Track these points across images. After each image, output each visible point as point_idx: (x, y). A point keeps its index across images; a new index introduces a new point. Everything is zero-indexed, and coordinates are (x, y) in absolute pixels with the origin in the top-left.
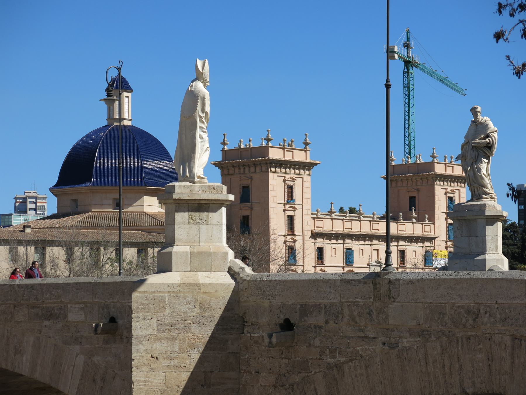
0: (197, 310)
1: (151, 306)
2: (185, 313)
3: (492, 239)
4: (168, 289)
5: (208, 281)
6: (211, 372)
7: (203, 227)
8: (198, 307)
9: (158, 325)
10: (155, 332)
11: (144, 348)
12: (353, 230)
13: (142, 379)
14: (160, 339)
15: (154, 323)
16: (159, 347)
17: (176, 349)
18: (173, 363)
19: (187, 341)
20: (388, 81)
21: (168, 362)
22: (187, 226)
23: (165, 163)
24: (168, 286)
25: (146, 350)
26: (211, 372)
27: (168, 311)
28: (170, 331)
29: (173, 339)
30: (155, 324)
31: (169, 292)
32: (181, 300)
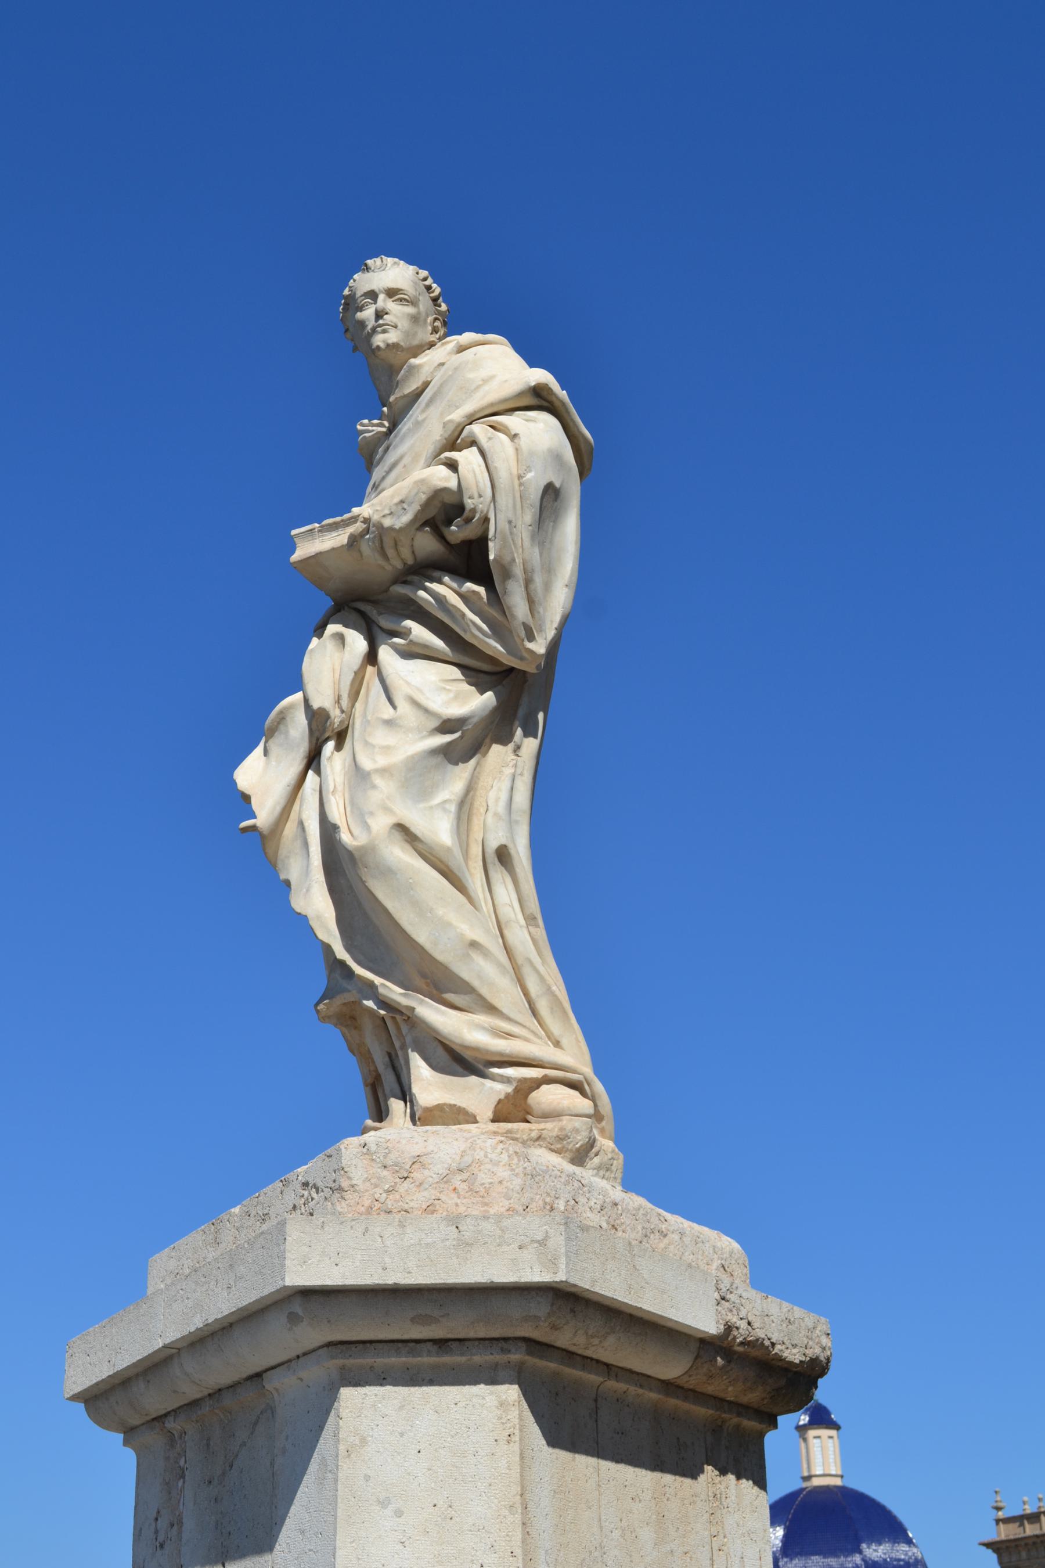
23: (904, 1547)
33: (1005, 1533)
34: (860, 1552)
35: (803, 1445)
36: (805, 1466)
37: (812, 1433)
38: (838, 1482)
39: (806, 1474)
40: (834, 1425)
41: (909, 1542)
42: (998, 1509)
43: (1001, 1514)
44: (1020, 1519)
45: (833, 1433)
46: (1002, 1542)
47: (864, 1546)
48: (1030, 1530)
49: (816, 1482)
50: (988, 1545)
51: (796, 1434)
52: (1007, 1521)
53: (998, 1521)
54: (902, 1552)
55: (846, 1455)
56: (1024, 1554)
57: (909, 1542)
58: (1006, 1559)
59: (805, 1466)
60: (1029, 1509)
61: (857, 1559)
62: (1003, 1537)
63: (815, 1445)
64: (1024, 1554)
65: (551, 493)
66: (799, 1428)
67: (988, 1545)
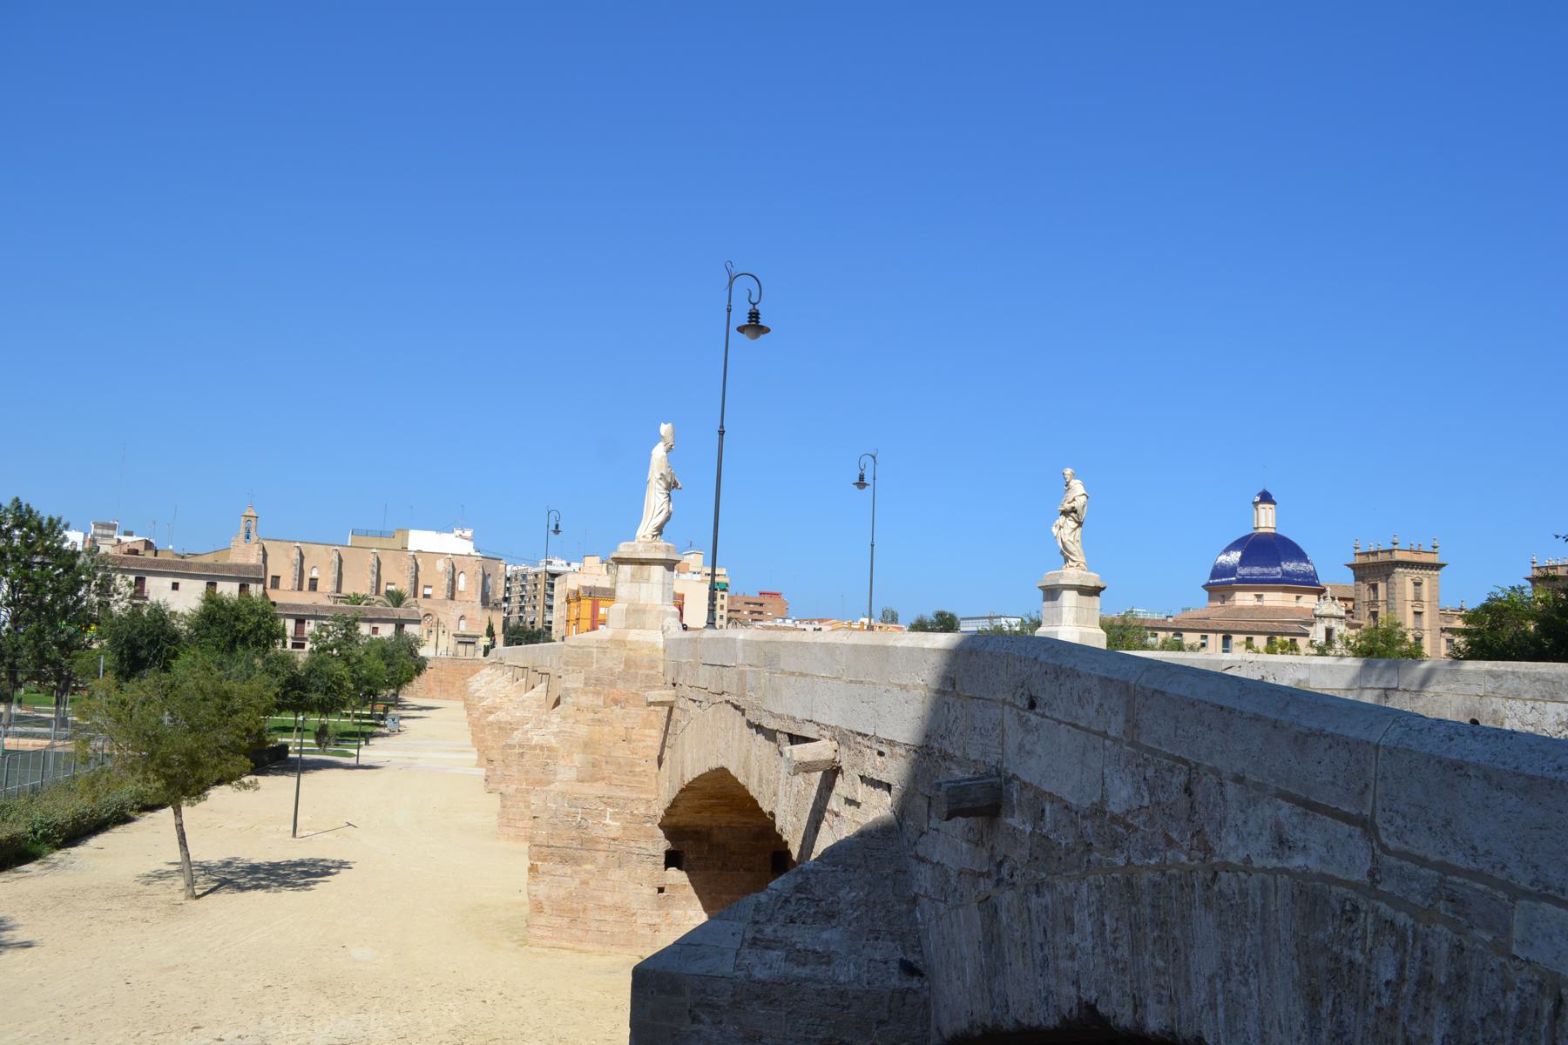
0: (622, 666)
1: (580, 660)
2: (611, 669)
3: (1069, 610)
4: (597, 645)
5: (640, 638)
6: (633, 728)
7: (644, 585)
8: (623, 664)
9: (586, 679)
10: (582, 686)
11: (571, 700)
12: (158, 558)
13: (569, 730)
14: (586, 693)
15: (582, 676)
16: (585, 700)
17: (601, 704)
18: (597, 716)
19: (611, 697)
20: (722, 427)
21: (591, 715)
22: (629, 585)
23: (1304, 564)
24: (597, 642)
25: (574, 704)
26: (633, 728)
27: (595, 666)
28: (596, 685)
29: (598, 694)
30: (583, 678)
31: (597, 647)
32: (608, 655)
33: (1359, 560)
34: (1280, 566)
35: (1255, 512)
36: (1256, 522)
37: (1261, 506)
38: (1273, 531)
39: (1256, 526)
40: (1274, 503)
41: (1308, 562)
42: (1356, 548)
43: (1358, 551)
44: (1367, 554)
45: (1273, 506)
46: (1356, 564)
47: (1283, 563)
48: (1372, 559)
49: (1261, 530)
50: (1348, 566)
51: (1252, 506)
52: (1360, 554)
53: (1355, 554)
54: (1303, 567)
55: (1278, 518)
56: (1367, 571)
57: (1308, 562)
58: (1357, 573)
59: (1256, 522)
60: (1372, 549)
61: (1278, 569)
62: (1357, 562)
63: (1262, 512)
64: (1367, 571)
65: (1084, 506)
66: (1254, 503)
67: (1348, 566)
